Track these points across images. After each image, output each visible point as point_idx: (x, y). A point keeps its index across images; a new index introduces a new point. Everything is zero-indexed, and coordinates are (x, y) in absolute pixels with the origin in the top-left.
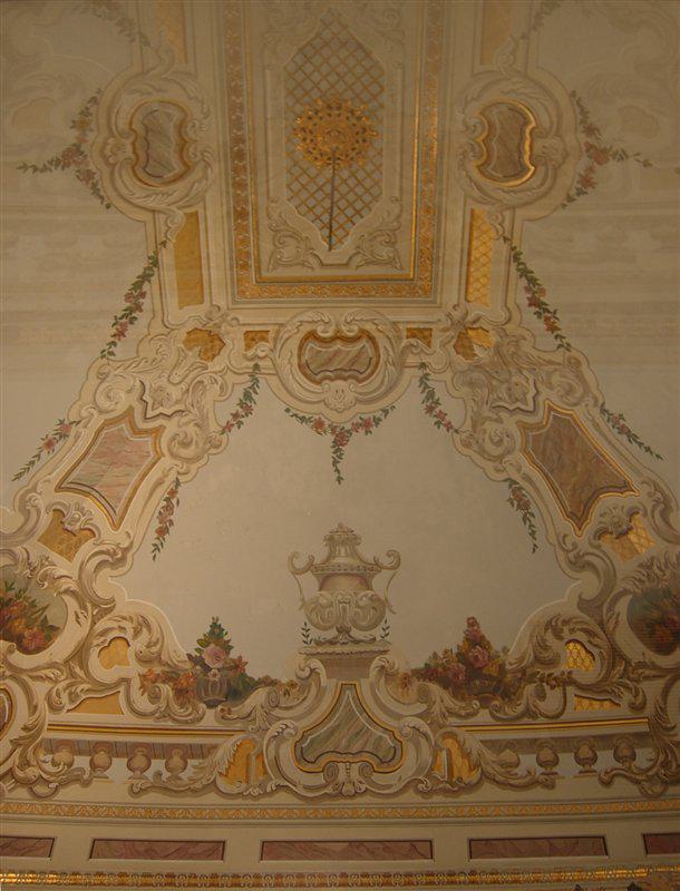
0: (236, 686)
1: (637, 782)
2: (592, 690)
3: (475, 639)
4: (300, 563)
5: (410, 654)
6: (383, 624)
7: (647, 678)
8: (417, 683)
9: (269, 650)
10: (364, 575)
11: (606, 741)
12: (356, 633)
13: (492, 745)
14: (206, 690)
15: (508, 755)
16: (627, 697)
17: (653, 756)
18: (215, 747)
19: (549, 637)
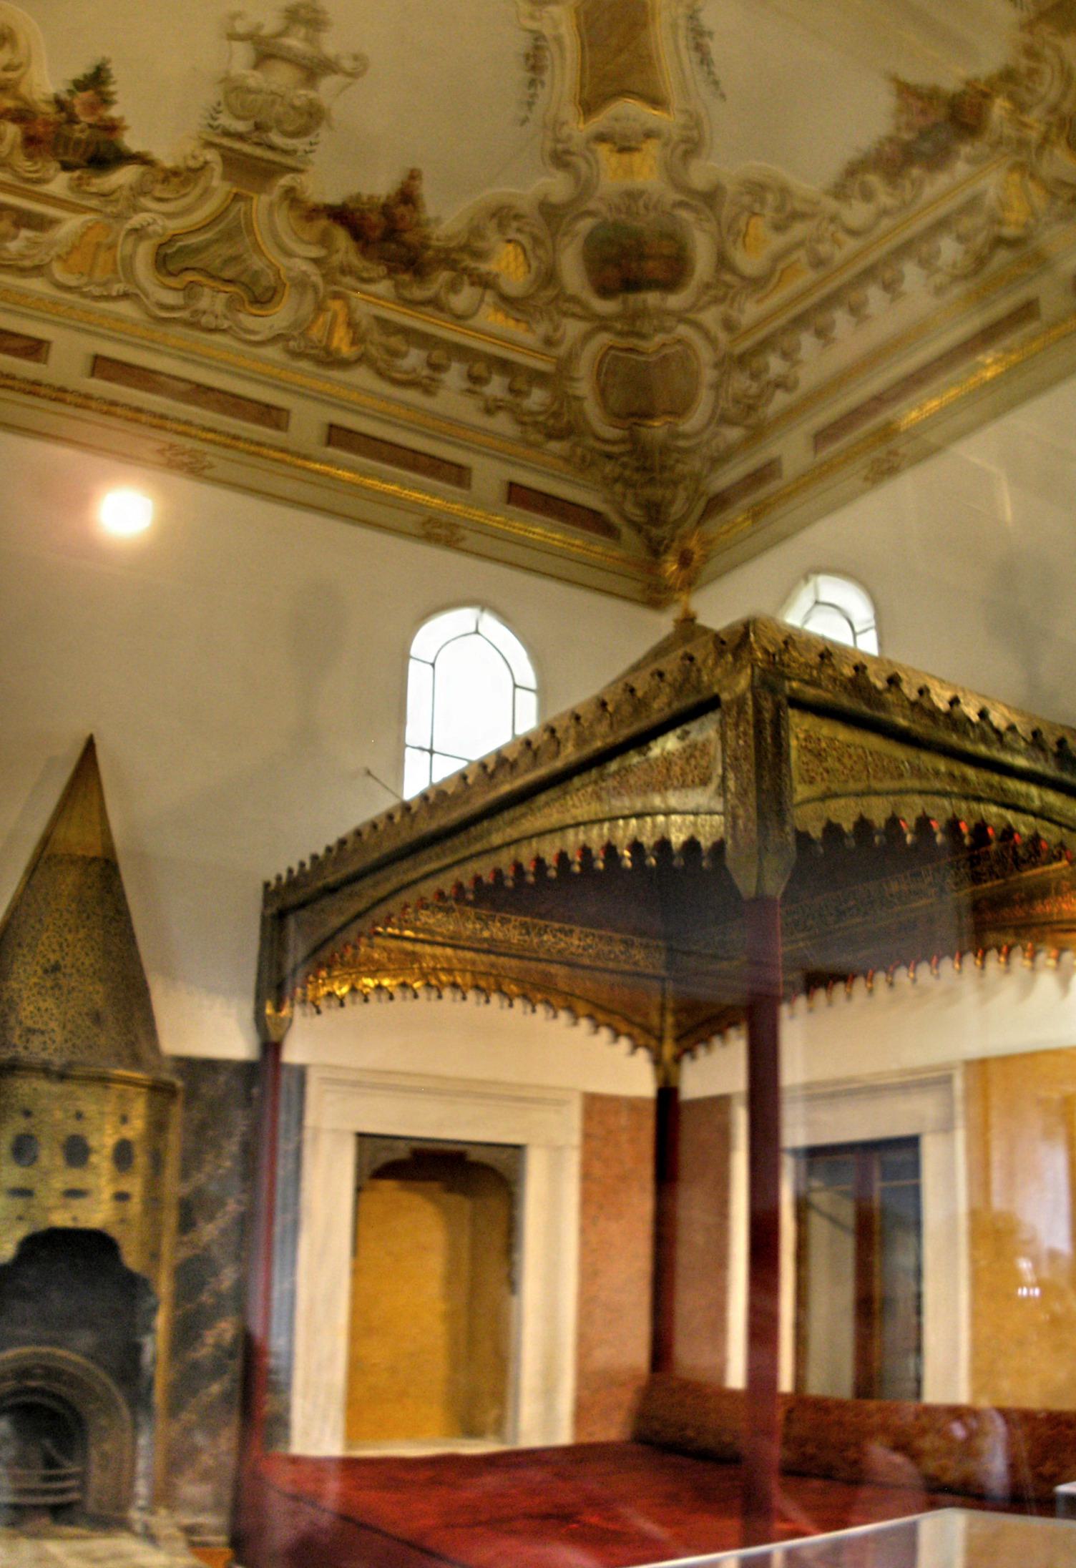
0: (103, 154)
1: (523, 423)
2: (508, 303)
3: (407, 196)
4: (241, 27)
5: (327, 182)
6: (311, 138)
7: (574, 315)
8: (323, 223)
9: (157, 122)
10: (313, 70)
11: (504, 366)
12: (276, 138)
13: (382, 323)
14: (66, 147)
15: (396, 342)
16: (543, 328)
17: (548, 401)
18: (53, 222)
19: (492, 225)
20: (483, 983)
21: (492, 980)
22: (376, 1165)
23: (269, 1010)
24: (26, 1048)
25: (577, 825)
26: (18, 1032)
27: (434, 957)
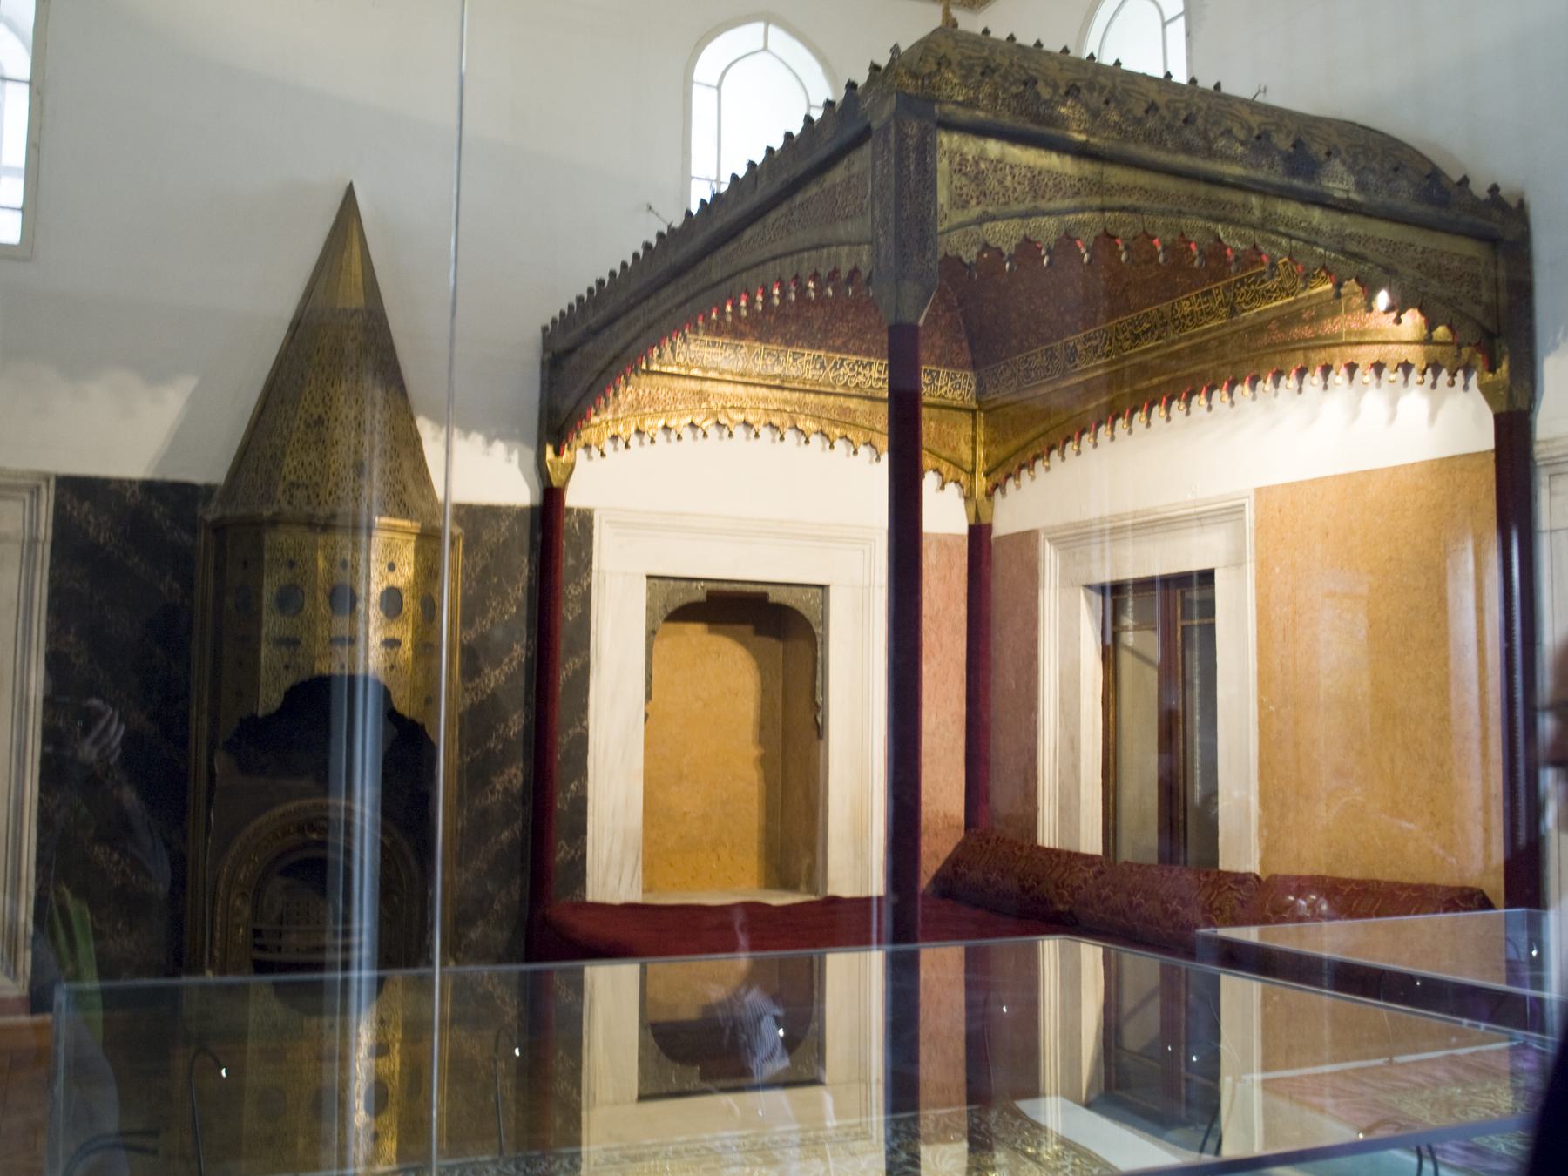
20: (776, 421)
21: (786, 416)
22: (670, 610)
23: (549, 451)
24: (290, 503)
25: (774, 258)
26: (281, 487)
27: (722, 396)
